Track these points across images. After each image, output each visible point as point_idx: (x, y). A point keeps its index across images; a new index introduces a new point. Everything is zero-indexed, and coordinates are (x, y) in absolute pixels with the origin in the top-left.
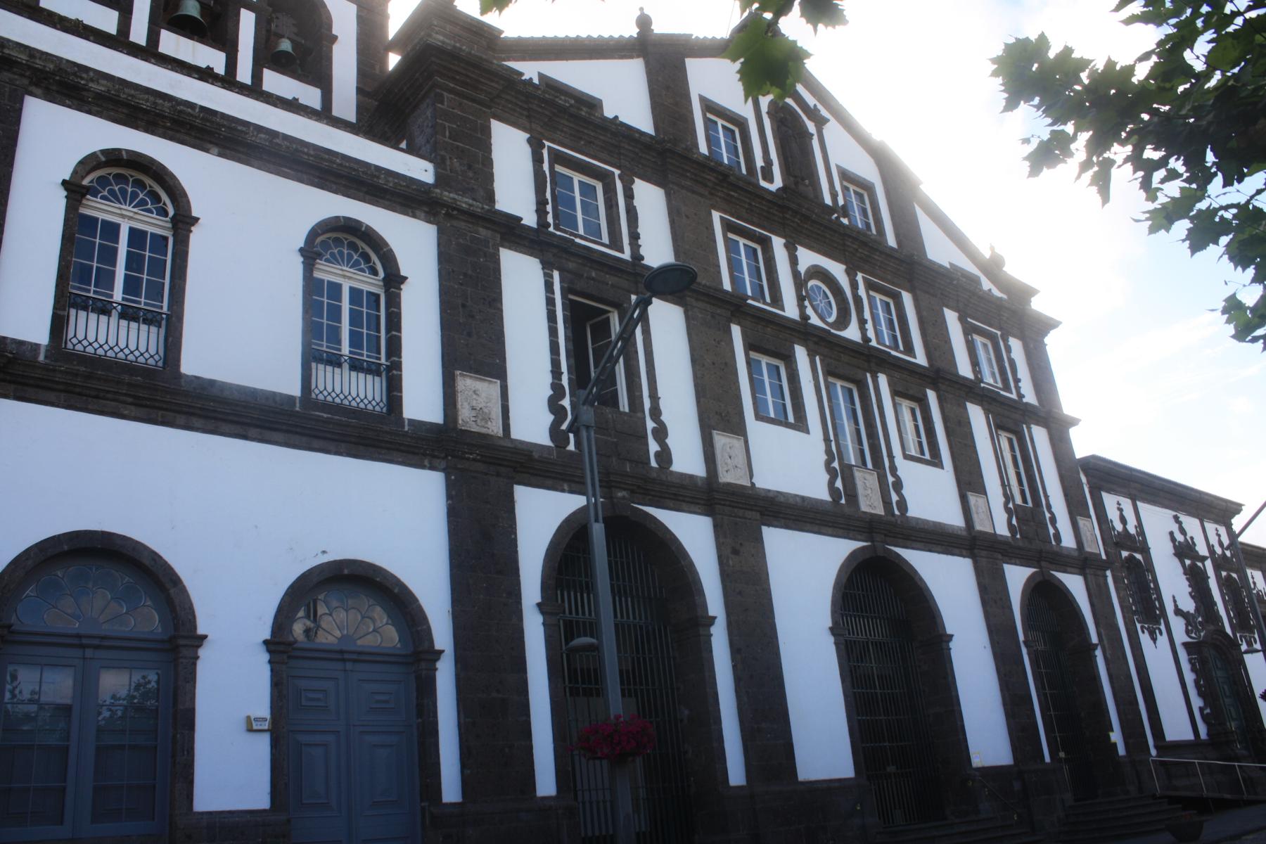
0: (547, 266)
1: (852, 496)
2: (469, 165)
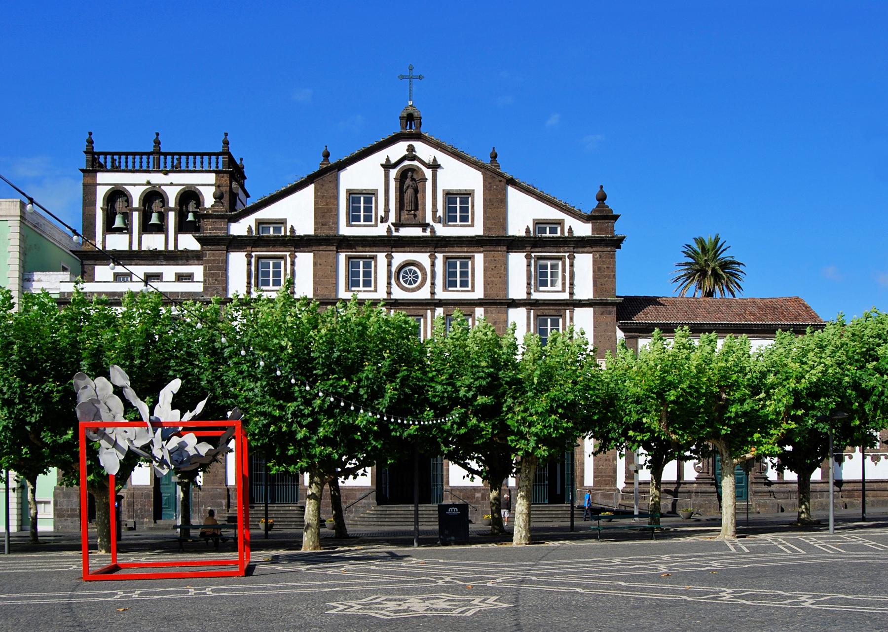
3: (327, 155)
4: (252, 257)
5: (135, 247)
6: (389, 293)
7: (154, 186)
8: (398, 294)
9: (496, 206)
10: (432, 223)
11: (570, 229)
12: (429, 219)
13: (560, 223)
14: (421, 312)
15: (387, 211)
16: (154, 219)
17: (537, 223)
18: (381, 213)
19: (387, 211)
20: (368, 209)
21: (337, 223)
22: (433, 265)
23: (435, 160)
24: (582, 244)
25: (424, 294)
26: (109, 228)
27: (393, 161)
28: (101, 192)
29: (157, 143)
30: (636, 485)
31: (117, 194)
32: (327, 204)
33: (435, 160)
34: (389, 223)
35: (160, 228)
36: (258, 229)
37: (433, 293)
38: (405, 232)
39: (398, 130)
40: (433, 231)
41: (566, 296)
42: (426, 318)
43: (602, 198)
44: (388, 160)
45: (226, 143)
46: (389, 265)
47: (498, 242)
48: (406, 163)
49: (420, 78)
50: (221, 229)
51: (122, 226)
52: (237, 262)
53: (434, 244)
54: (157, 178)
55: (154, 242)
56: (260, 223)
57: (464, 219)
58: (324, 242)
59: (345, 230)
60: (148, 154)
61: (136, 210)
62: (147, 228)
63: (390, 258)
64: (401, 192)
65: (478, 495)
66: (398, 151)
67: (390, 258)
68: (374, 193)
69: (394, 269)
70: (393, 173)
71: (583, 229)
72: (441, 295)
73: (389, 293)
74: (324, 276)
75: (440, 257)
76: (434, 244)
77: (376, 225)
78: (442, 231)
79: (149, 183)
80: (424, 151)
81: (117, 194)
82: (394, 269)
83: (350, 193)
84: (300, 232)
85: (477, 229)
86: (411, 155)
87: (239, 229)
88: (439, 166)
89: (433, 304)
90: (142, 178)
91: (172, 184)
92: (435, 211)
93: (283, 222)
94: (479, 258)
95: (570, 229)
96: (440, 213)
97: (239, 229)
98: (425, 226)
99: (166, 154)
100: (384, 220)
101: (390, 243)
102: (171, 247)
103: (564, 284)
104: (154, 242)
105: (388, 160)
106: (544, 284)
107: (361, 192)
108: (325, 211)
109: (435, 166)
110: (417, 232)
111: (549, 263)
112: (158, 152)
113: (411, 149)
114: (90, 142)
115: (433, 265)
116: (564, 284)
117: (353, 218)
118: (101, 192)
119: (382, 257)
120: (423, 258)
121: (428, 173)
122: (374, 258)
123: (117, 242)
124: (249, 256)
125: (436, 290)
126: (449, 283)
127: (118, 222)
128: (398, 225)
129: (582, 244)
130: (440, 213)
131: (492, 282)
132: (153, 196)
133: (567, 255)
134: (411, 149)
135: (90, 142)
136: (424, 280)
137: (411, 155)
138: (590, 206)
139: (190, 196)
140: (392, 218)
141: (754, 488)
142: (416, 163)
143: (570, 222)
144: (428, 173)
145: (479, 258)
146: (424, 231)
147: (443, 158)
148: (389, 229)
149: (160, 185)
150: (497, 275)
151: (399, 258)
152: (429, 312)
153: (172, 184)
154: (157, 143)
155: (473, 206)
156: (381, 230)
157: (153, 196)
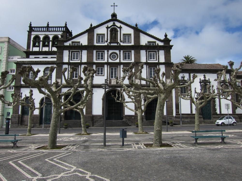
0: (69, 65)
1: (110, 83)
2: (61, 57)
3: (91, 25)
4: (70, 51)
5: (41, 50)
6: (108, 61)
7: (46, 35)
8: (110, 61)
9: (137, 38)
10: (120, 42)
11: (158, 44)
12: (119, 41)
13: (155, 42)
14: (117, 66)
15: (107, 39)
16: (46, 44)
17: (149, 42)
18: (106, 40)
19: (107, 39)
20: (102, 39)
21: (93, 42)
22: (120, 53)
23: (120, 26)
24: (160, 48)
25: (118, 61)
26: (34, 46)
27: (109, 26)
28: (32, 37)
29: (48, 24)
30: (181, 115)
31: (37, 38)
32: (91, 37)
33: (120, 26)
34: (108, 42)
35: (48, 46)
36: (72, 44)
37: (120, 61)
38: (112, 44)
39: (111, 18)
40: (120, 44)
41: (157, 61)
42: (118, 68)
43: (166, 36)
44: (108, 26)
45: (66, 24)
46: (108, 53)
47: (138, 47)
48: (113, 27)
49: (117, 6)
50: (62, 44)
51: (38, 45)
52: (66, 53)
53: (120, 48)
54: (47, 33)
55: (46, 49)
56: (73, 42)
57: (128, 41)
58: (90, 48)
59: (96, 44)
60: (45, 27)
61: (41, 41)
62: (44, 45)
63: (108, 51)
64: (111, 34)
65: (133, 118)
66: (110, 24)
67: (108, 51)
68: (104, 35)
69: (109, 54)
70: (109, 29)
71: (161, 44)
72: (122, 61)
73: (108, 61)
74: (90, 56)
75: (122, 51)
76: (120, 48)
77: (104, 43)
78: (122, 44)
79: (45, 34)
80: (118, 24)
81: (37, 38)
82: (109, 54)
83: (97, 34)
84: (83, 45)
85: (132, 44)
86: (114, 25)
87: (67, 44)
88: (122, 27)
89: (120, 64)
90: (44, 33)
91: (51, 35)
92: (120, 39)
93: (79, 42)
94: (133, 52)
95: (158, 44)
96: (122, 40)
97: (67, 44)
98: (118, 43)
99: (50, 27)
100: (107, 42)
101: (108, 48)
102: (50, 50)
103: (156, 58)
104: (46, 49)
105: (108, 26)
106: (151, 58)
107: (101, 34)
108: (90, 39)
109: (120, 28)
110: (116, 44)
111: (152, 53)
112: (48, 27)
113: (114, 23)
114: (31, 24)
115: (120, 53)
116: (156, 58)
117: (98, 41)
118: (32, 37)
119: (106, 51)
120: (117, 52)
121: (119, 30)
122: (104, 52)
123: (36, 49)
124: (69, 52)
125: (121, 60)
126: (125, 58)
127: (37, 44)
128: (110, 43)
129: (160, 48)
130: (122, 40)
131: (136, 58)
132: (46, 38)
133: (157, 51)
134: (114, 23)
135: (31, 24)
136: (118, 57)
137: (114, 25)
138: (162, 38)
139: (55, 37)
140: (109, 41)
141: (214, 116)
142: (115, 27)
143: (157, 42)
144: (119, 30)
145: (133, 52)
146: (118, 44)
147: (123, 26)
148: (108, 44)
149: (48, 35)
150: (138, 56)
151: (111, 52)
152: (119, 66)
153: (51, 35)
154: (48, 24)
155: (131, 38)
156: (106, 44)
157: (46, 38)
